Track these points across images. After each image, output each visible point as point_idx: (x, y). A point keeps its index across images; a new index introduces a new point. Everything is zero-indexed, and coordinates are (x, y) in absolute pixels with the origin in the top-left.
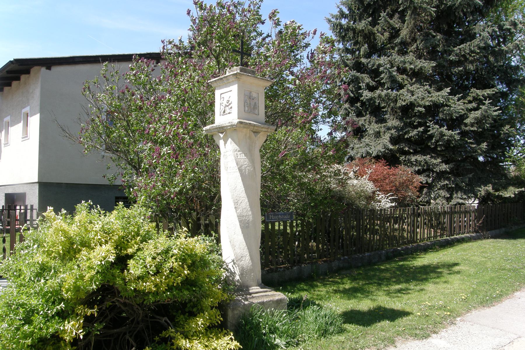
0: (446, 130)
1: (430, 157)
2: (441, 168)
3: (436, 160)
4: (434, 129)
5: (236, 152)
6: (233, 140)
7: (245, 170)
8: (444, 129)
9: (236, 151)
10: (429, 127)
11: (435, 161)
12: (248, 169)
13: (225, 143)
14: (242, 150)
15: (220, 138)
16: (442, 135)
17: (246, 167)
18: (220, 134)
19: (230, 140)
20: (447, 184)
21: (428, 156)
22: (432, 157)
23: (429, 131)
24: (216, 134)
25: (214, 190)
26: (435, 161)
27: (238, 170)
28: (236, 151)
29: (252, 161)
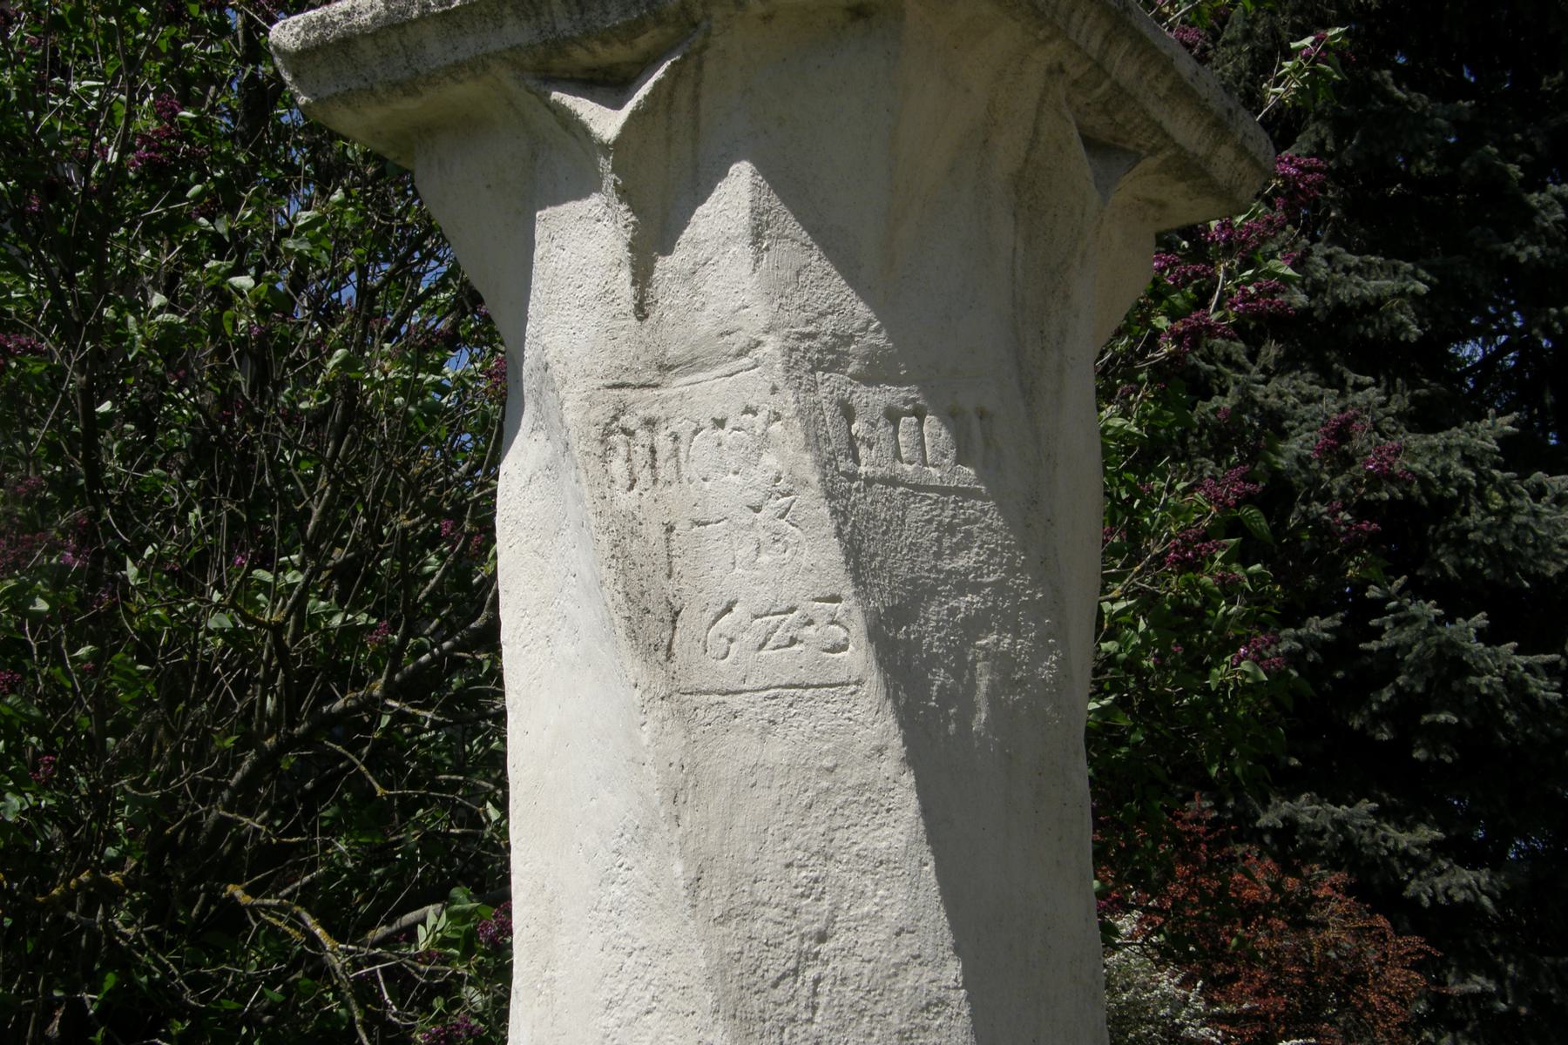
0: (1481, 635)
1: (1374, 813)
2: (1440, 883)
3: (1411, 828)
4: (1411, 625)
5: (830, 385)
6: (789, 182)
7: (962, 669)
8: (1467, 629)
9: (832, 357)
10: (1378, 607)
11: (1404, 840)
12: (1002, 662)
13: (653, 236)
14: (920, 361)
15: (564, 167)
16: (1450, 666)
17: (975, 624)
18: (585, 108)
19: (737, 190)
20: (1484, 995)
21: (1365, 806)
22: (1381, 814)
23: (1377, 633)
24: (467, 126)
25: (474, 997)
26: (1404, 840)
27: (858, 658)
28: (832, 357)
29: (1030, 515)
